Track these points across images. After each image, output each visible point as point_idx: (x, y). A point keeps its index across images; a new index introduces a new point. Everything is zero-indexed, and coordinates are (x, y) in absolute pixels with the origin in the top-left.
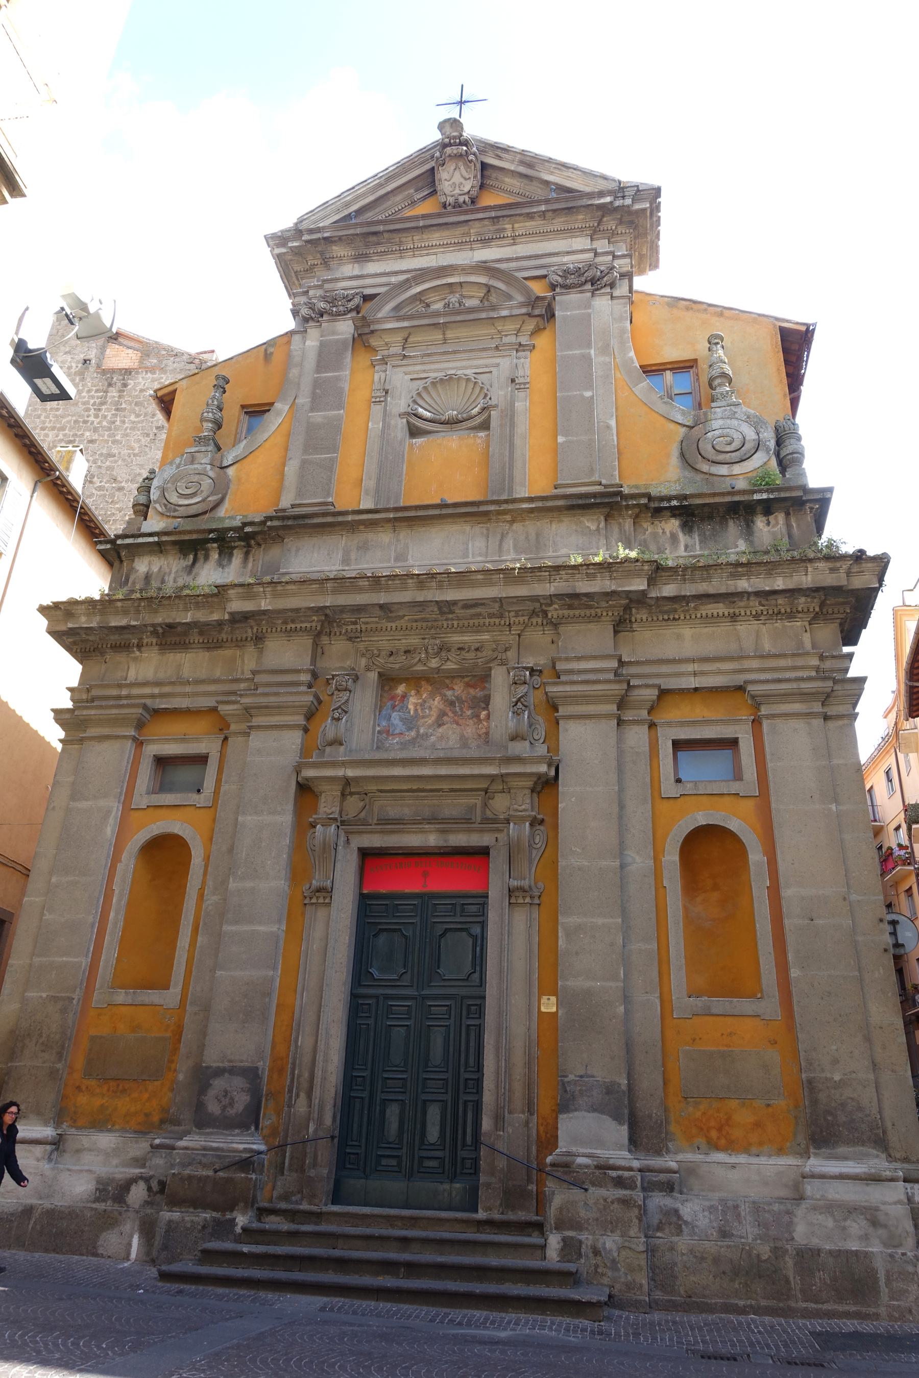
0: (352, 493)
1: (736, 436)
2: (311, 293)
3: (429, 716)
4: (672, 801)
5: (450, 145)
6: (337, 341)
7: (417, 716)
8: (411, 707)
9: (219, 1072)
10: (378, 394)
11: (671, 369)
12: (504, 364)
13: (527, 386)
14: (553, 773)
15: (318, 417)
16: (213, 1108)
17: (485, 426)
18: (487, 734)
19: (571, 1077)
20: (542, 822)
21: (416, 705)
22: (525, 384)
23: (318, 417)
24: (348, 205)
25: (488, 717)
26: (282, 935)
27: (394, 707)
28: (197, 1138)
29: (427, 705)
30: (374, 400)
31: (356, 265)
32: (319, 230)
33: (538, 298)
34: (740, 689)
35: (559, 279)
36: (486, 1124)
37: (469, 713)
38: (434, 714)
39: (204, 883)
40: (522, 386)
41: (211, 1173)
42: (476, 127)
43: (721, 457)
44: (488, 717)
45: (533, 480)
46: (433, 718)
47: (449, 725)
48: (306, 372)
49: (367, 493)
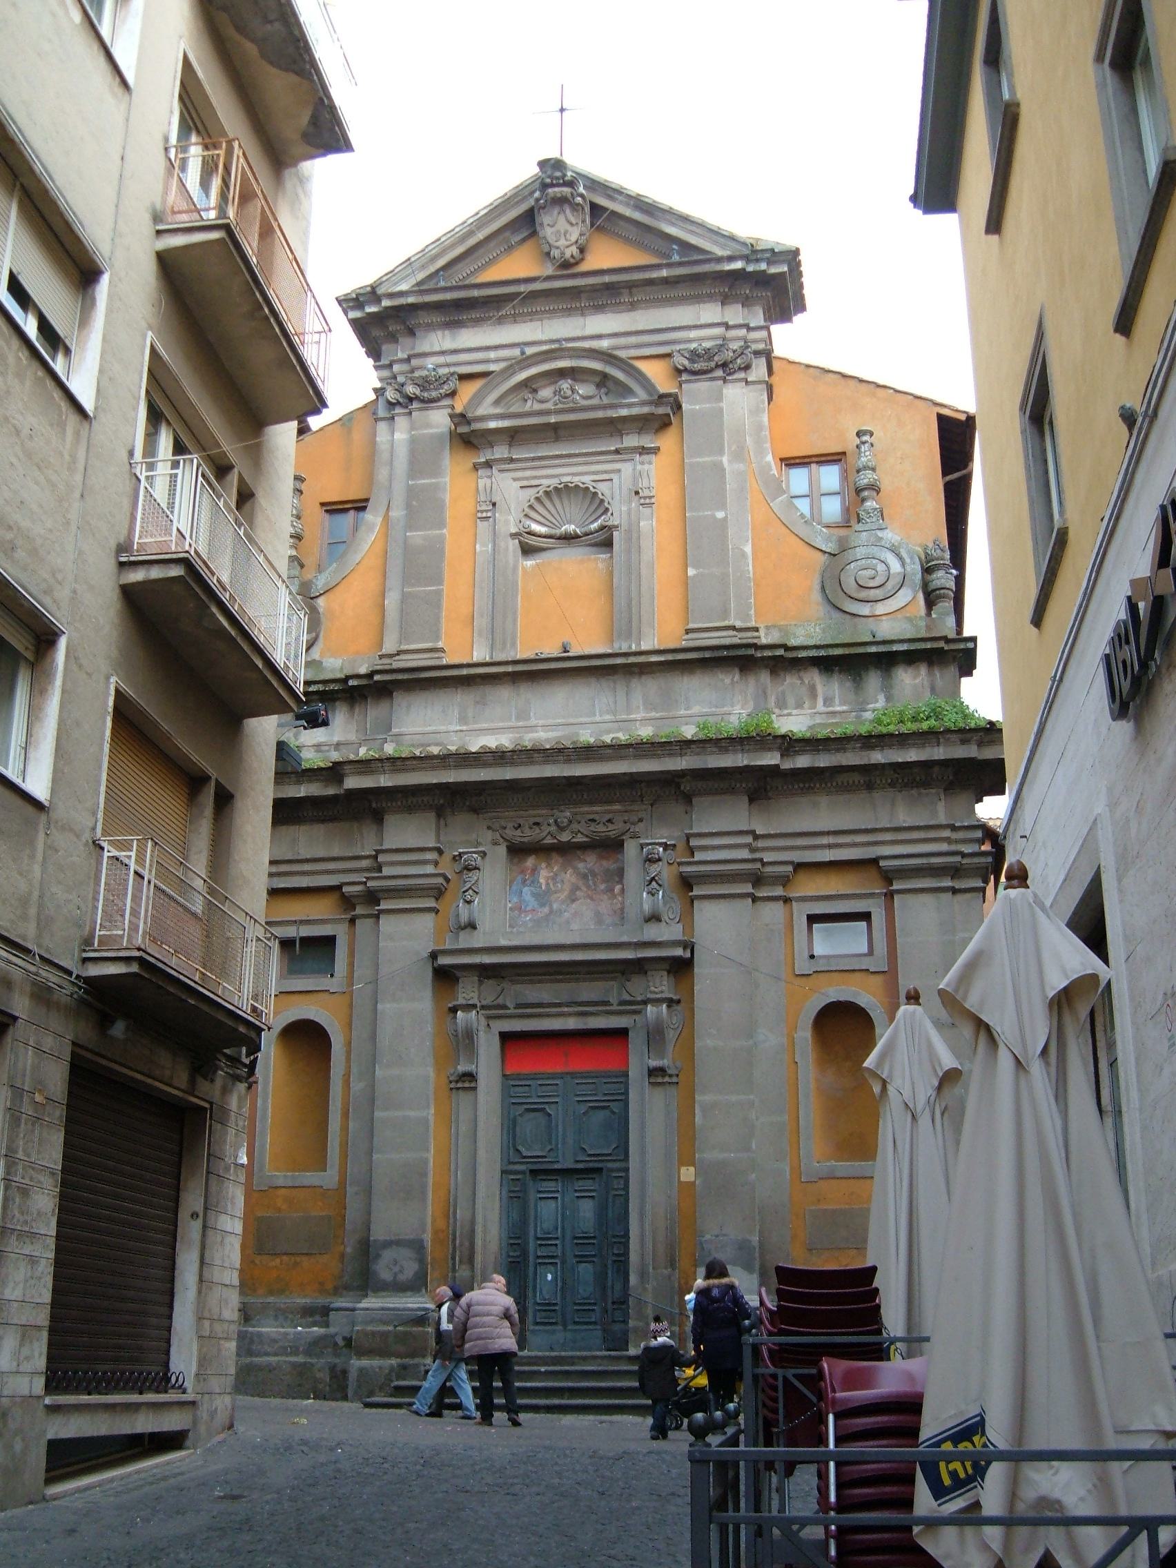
0: (465, 647)
1: (881, 568)
2: (396, 368)
3: (561, 891)
5: (552, 185)
6: (432, 436)
8: (542, 881)
9: (388, 1244)
10: (484, 508)
11: (817, 462)
13: (653, 500)
14: (688, 955)
15: (417, 536)
16: (385, 1275)
17: (607, 544)
18: (622, 909)
19: (708, 1237)
20: (679, 1002)
21: (548, 878)
22: (650, 497)
23: (417, 536)
24: (434, 259)
25: (623, 890)
26: (431, 1119)
27: (524, 881)
28: (374, 1300)
30: (479, 515)
31: (447, 332)
32: (401, 294)
33: (662, 396)
34: (874, 862)
35: (686, 362)
36: (633, 1279)
37: (603, 887)
38: (567, 887)
39: (348, 1067)
40: (648, 501)
41: (391, 1328)
42: (580, 160)
43: (863, 594)
44: (623, 890)
45: (661, 632)
46: (566, 893)
48: (395, 474)
49: (480, 635)
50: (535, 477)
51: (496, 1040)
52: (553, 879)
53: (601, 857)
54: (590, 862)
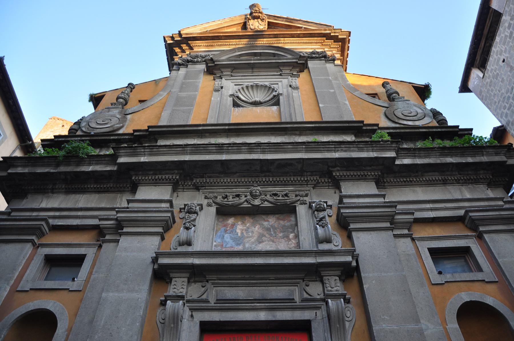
4: (439, 287)
7: (242, 237)
12: (285, 81)
21: (242, 230)
29: (250, 230)
46: (255, 238)
47: (267, 242)
50: (242, 82)
51: (197, 329)
52: (246, 230)
53: (278, 219)
54: (272, 221)
